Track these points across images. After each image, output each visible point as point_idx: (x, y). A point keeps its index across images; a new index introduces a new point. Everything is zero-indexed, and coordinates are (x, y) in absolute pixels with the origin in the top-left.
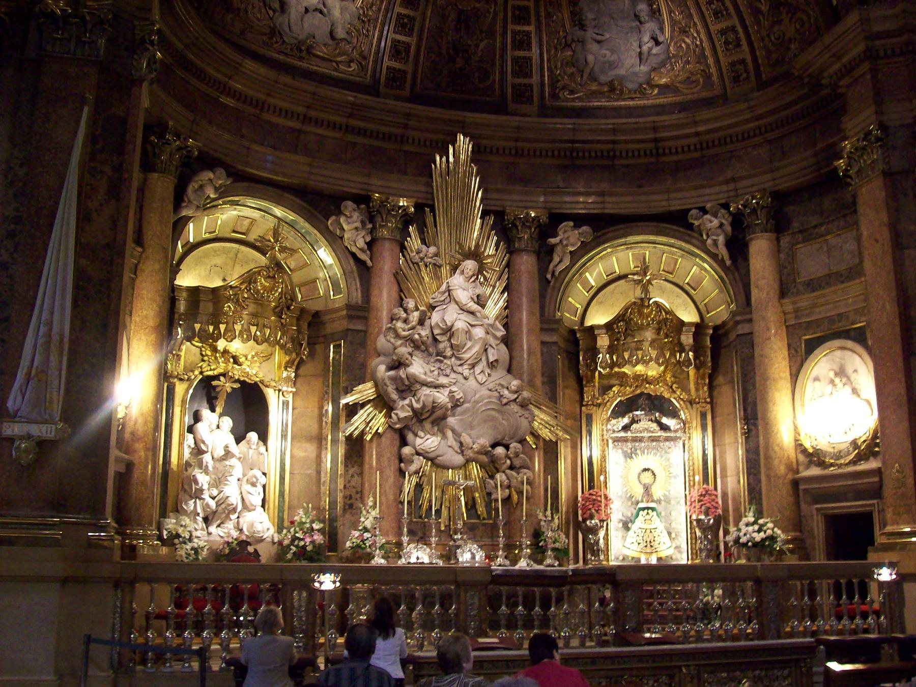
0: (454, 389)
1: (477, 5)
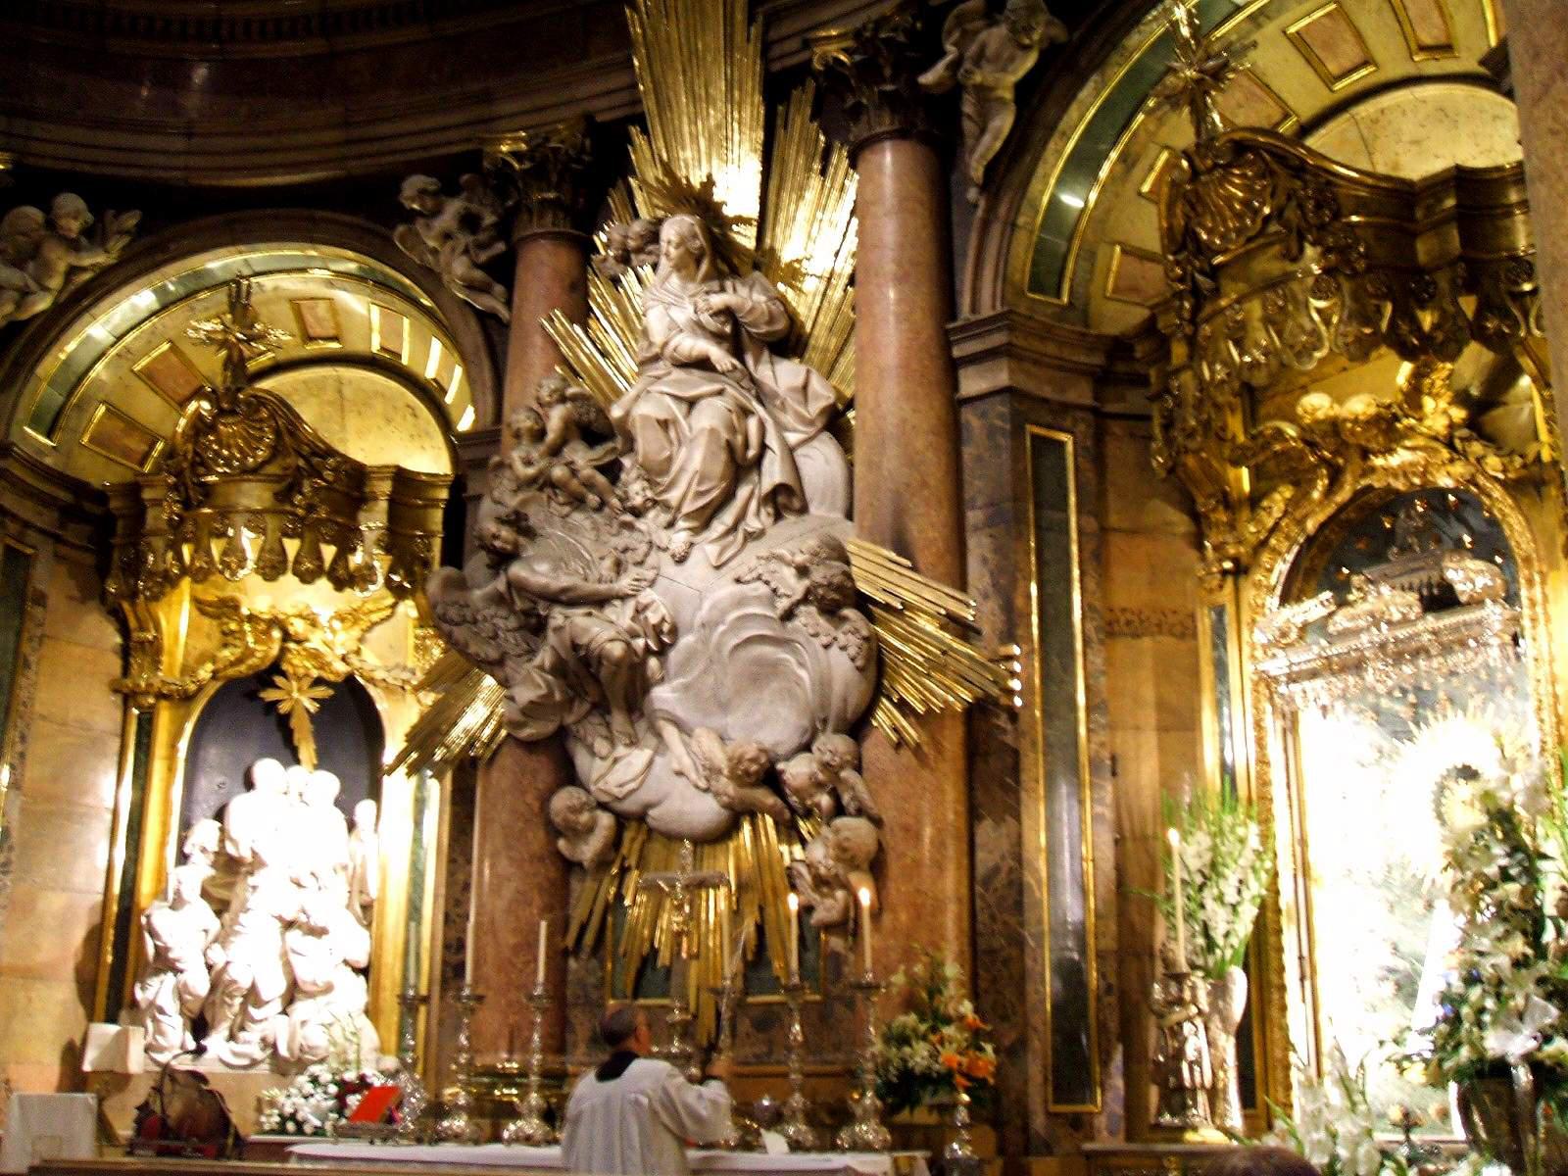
0: (648, 595)
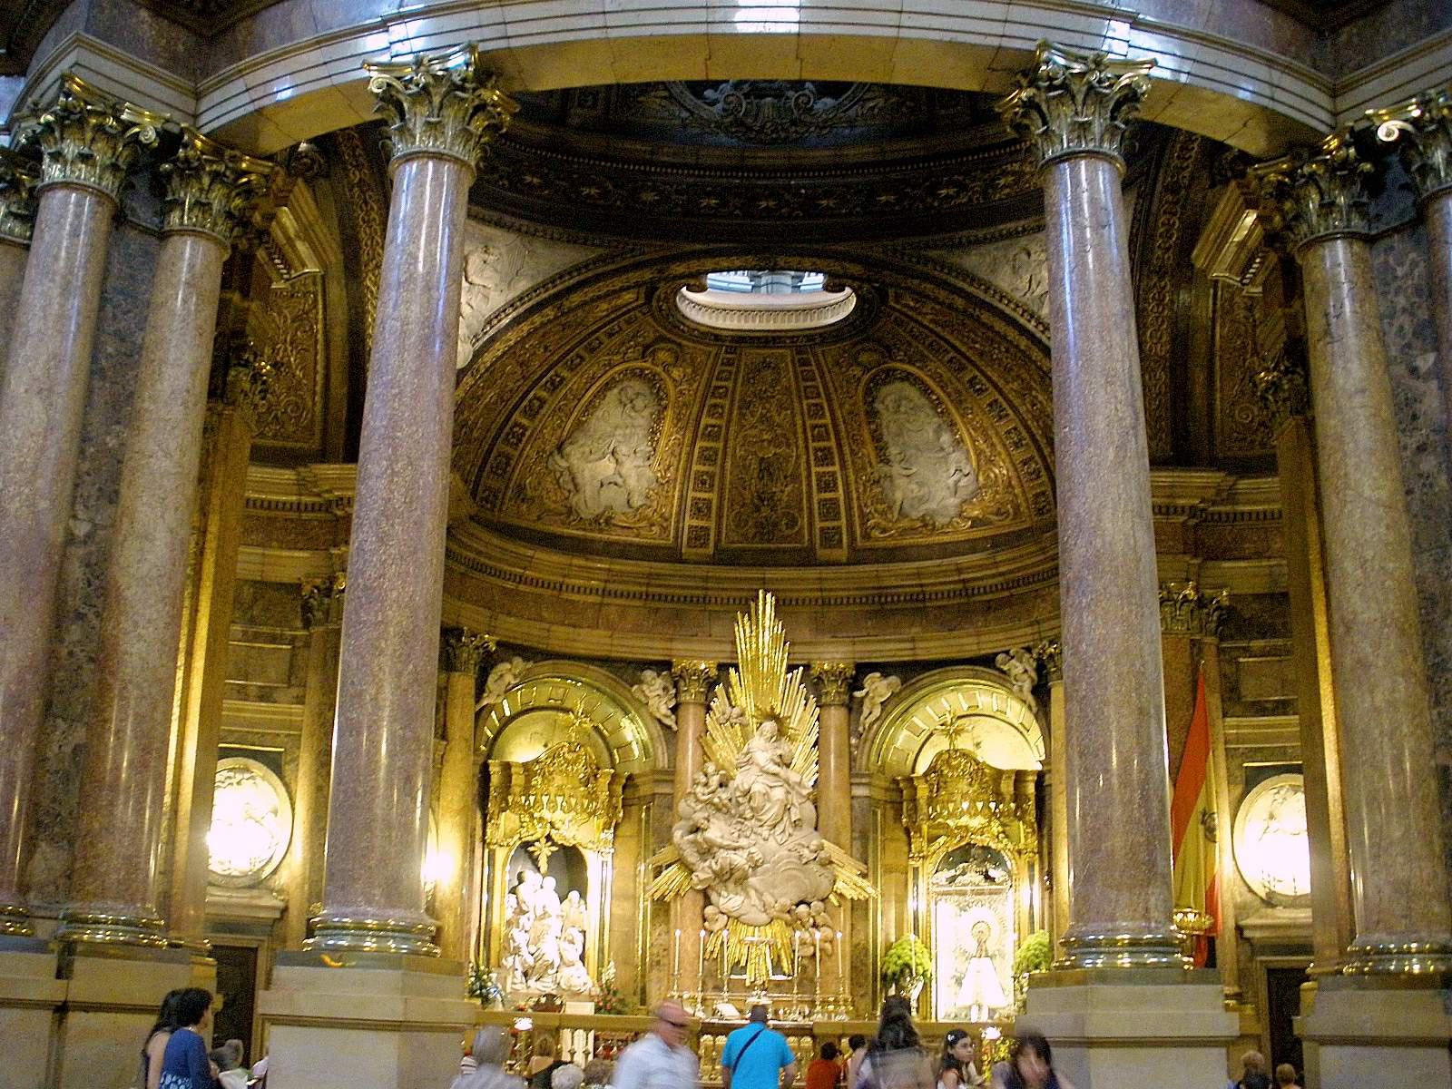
1: (778, 451)
